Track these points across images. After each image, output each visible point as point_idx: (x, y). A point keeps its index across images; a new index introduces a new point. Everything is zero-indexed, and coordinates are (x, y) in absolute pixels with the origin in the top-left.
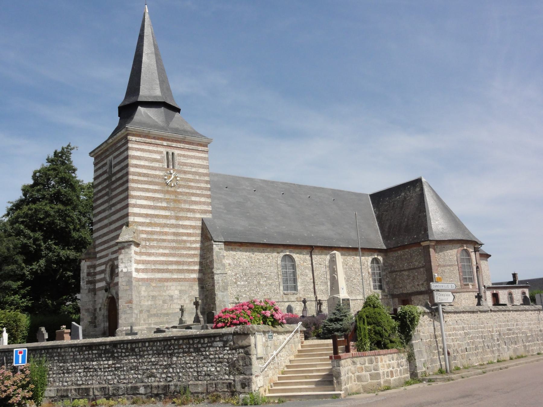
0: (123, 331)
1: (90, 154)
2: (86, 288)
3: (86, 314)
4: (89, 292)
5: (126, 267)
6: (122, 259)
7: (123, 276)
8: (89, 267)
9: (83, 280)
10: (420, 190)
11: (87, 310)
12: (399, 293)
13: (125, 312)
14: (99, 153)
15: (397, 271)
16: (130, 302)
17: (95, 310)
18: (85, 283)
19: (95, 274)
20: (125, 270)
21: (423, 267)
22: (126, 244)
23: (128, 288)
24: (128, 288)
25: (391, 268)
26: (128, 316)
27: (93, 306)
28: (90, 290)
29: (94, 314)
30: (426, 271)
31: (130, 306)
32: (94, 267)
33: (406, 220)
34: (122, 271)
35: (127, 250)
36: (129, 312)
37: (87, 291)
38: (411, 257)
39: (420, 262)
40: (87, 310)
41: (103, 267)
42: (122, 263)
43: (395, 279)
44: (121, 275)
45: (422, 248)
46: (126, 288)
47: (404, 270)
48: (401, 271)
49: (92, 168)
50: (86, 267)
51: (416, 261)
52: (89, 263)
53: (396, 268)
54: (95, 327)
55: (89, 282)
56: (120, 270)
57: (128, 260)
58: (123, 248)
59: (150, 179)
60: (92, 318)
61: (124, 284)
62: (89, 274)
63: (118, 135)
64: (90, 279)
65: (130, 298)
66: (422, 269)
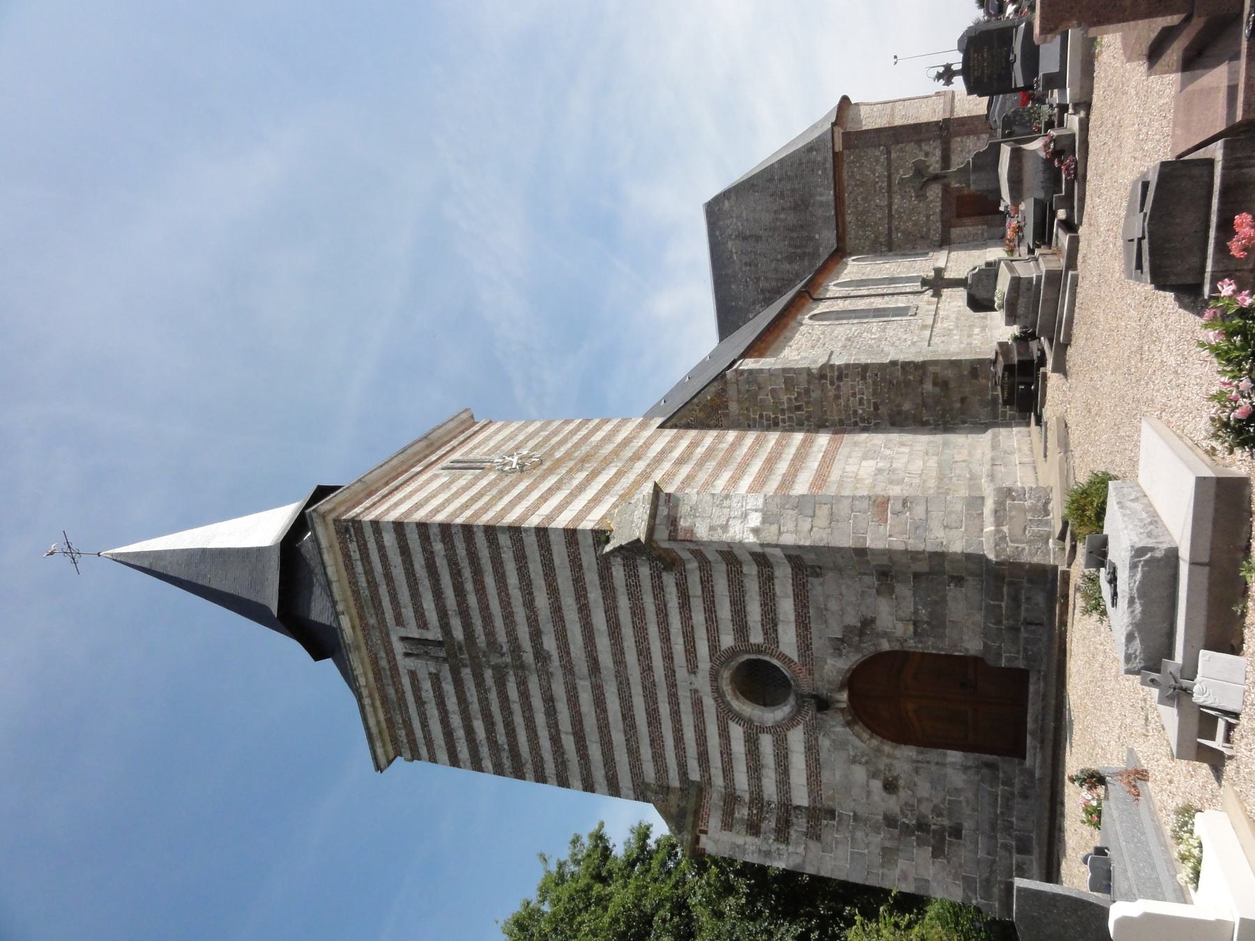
0: (998, 531)
1: (379, 768)
2: (801, 849)
3: (902, 864)
4: (818, 838)
5: (745, 516)
6: (712, 528)
7: (774, 528)
8: (727, 825)
9: (768, 854)
10: (728, 199)
11: (888, 855)
12: (939, 225)
13: (921, 526)
14: (382, 716)
15: (890, 229)
16: (880, 505)
17: (890, 821)
18: (782, 847)
19: (757, 799)
20: (755, 520)
21: (889, 153)
22: (663, 511)
23: (823, 512)
24: (823, 512)
25: (881, 244)
26: (937, 514)
27: (877, 830)
28: (814, 834)
29: (907, 830)
30: (897, 143)
31: (899, 507)
32: (731, 799)
33: (782, 216)
34: (756, 531)
35: (684, 509)
36: (920, 511)
37: (813, 845)
38: (863, 184)
39: (877, 161)
40: (888, 855)
41: (737, 731)
42: (725, 528)
43: (906, 234)
44: (770, 535)
45: (846, 152)
46: (822, 521)
47: (890, 205)
48: (890, 216)
49: (422, 767)
50: (727, 837)
51: (873, 172)
52: (714, 821)
53: (883, 229)
54: (957, 832)
55: (782, 833)
56: (751, 539)
57: (720, 506)
58: (673, 521)
59: (494, 491)
60: (921, 843)
61: (806, 525)
62: (754, 828)
63: (359, 671)
64: (770, 824)
65: (865, 505)
66: (893, 155)
